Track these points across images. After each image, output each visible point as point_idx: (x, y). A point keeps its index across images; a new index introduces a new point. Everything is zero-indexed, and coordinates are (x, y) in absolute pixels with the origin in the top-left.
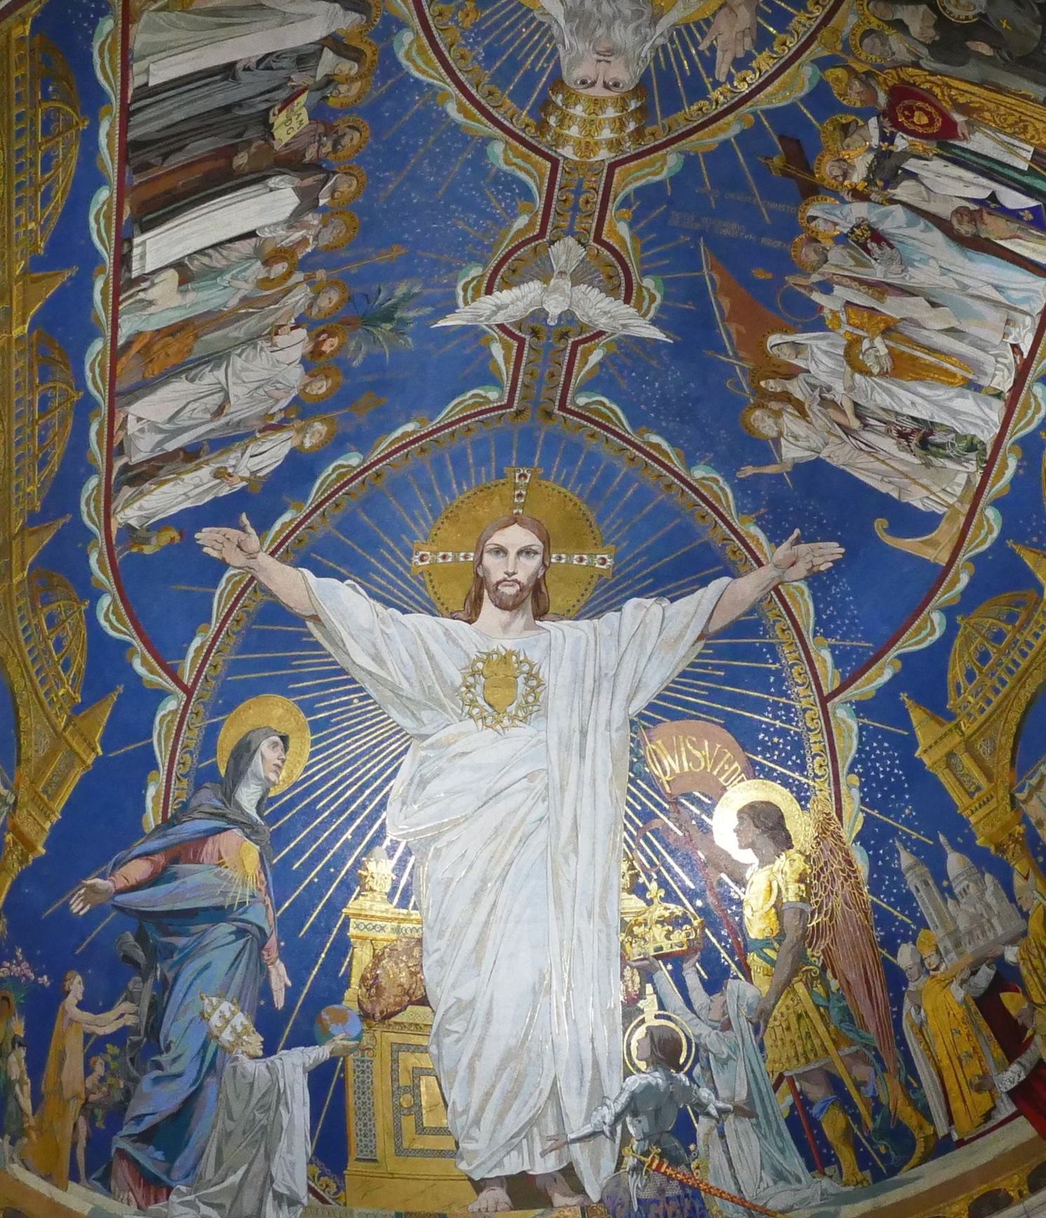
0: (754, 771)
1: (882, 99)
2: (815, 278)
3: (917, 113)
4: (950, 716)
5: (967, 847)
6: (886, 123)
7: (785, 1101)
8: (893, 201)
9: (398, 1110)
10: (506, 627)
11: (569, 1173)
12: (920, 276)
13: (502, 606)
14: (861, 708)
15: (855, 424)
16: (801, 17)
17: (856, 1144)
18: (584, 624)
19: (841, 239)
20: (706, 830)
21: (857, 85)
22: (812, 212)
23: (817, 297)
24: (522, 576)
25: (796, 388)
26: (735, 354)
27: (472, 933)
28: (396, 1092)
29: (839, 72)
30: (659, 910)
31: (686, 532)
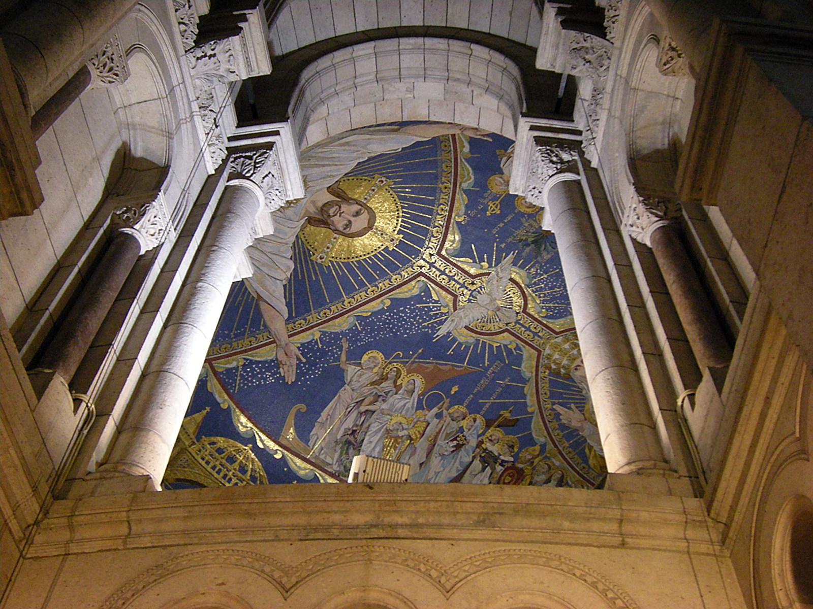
1: (520, 466)
2: (445, 412)
3: (510, 479)
4: (199, 439)
6: (510, 465)
8: (474, 458)
10: (313, 202)
12: (435, 461)
15: (363, 409)
16: (567, 444)
18: (293, 239)
19: (461, 430)
21: (530, 457)
22: (478, 421)
23: (435, 410)
24: (336, 219)
25: (387, 385)
26: (416, 362)
29: (537, 453)
31: (320, 303)
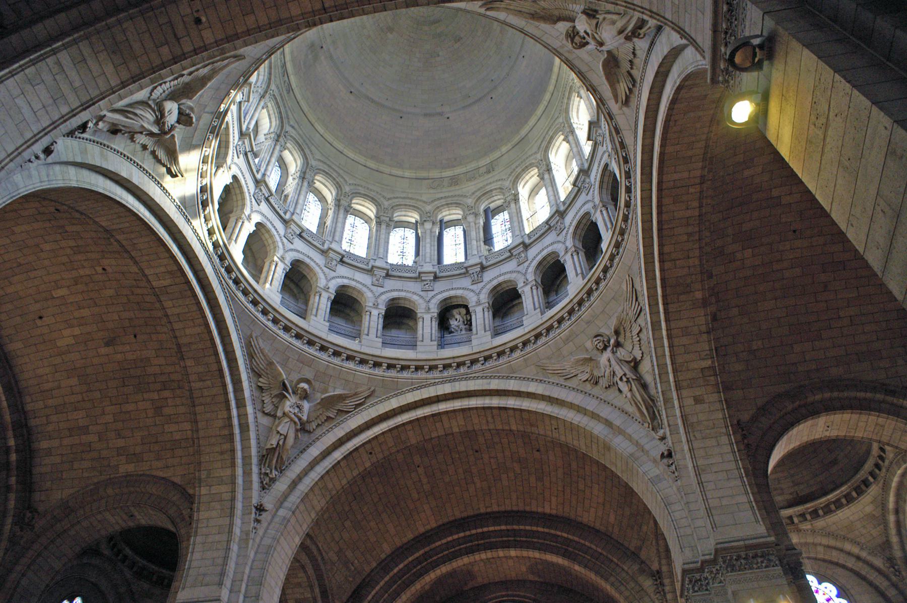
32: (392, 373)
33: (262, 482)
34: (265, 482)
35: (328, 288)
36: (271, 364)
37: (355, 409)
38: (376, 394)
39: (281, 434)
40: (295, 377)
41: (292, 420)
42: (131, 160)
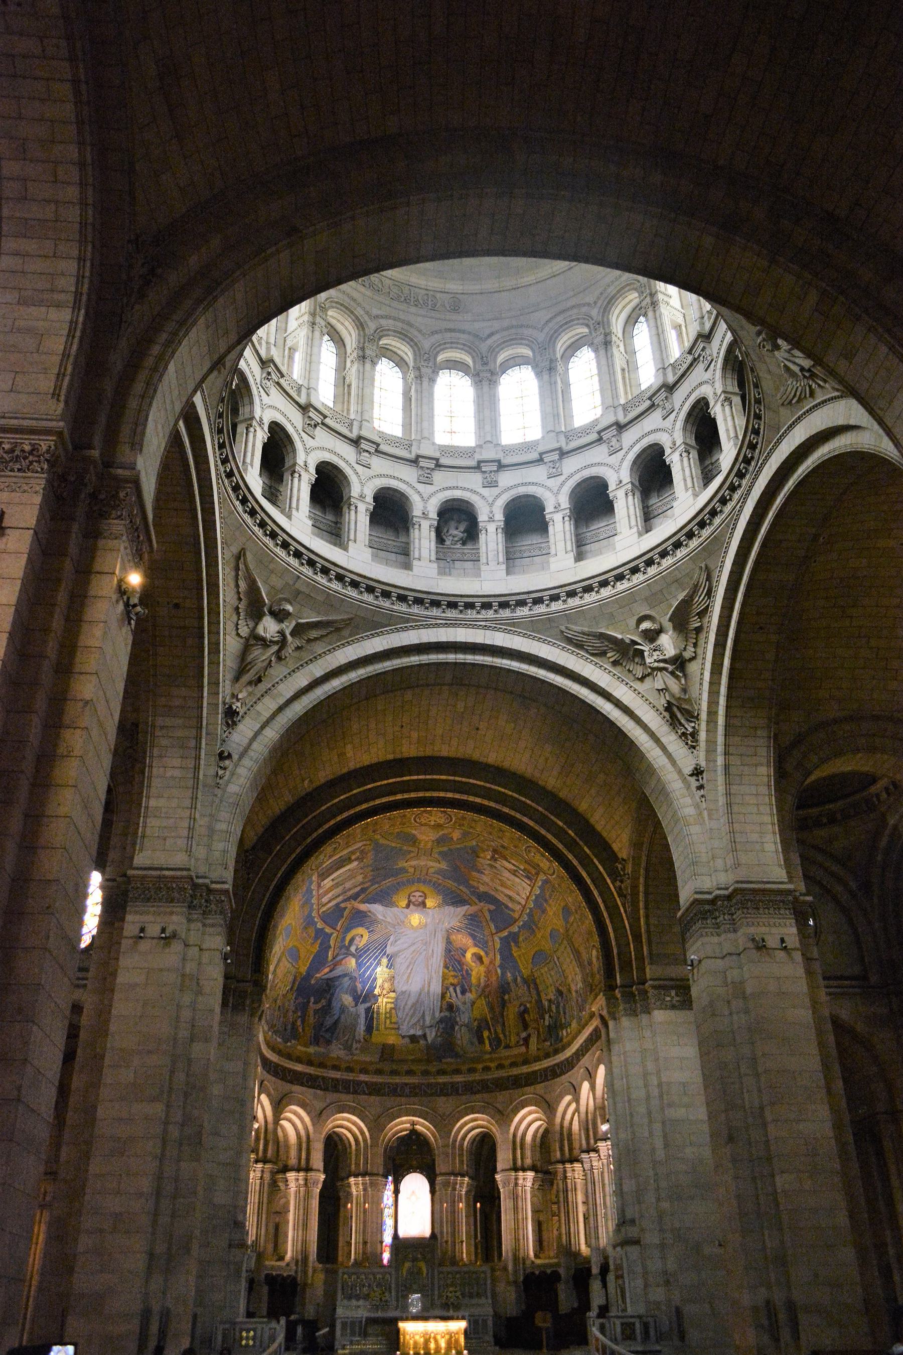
0: (476, 945)
5: (522, 977)
7: (476, 1024)
9: (386, 1018)
11: (425, 1036)
13: (415, 905)
14: (501, 939)
17: (490, 1040)
20: (464, 956)
27: (406, 975)
28: (386, 1013)
30: (452, 973)
32: (706, 532)
33: (687, 744)
34: (689, 742)
35: (621, 482)
36: (602, 636)
37: (709, 598)
38: (712, 567)
39: (662, 690)
40: (633, 622)
41: (661, 669)
42: (302, 665)
